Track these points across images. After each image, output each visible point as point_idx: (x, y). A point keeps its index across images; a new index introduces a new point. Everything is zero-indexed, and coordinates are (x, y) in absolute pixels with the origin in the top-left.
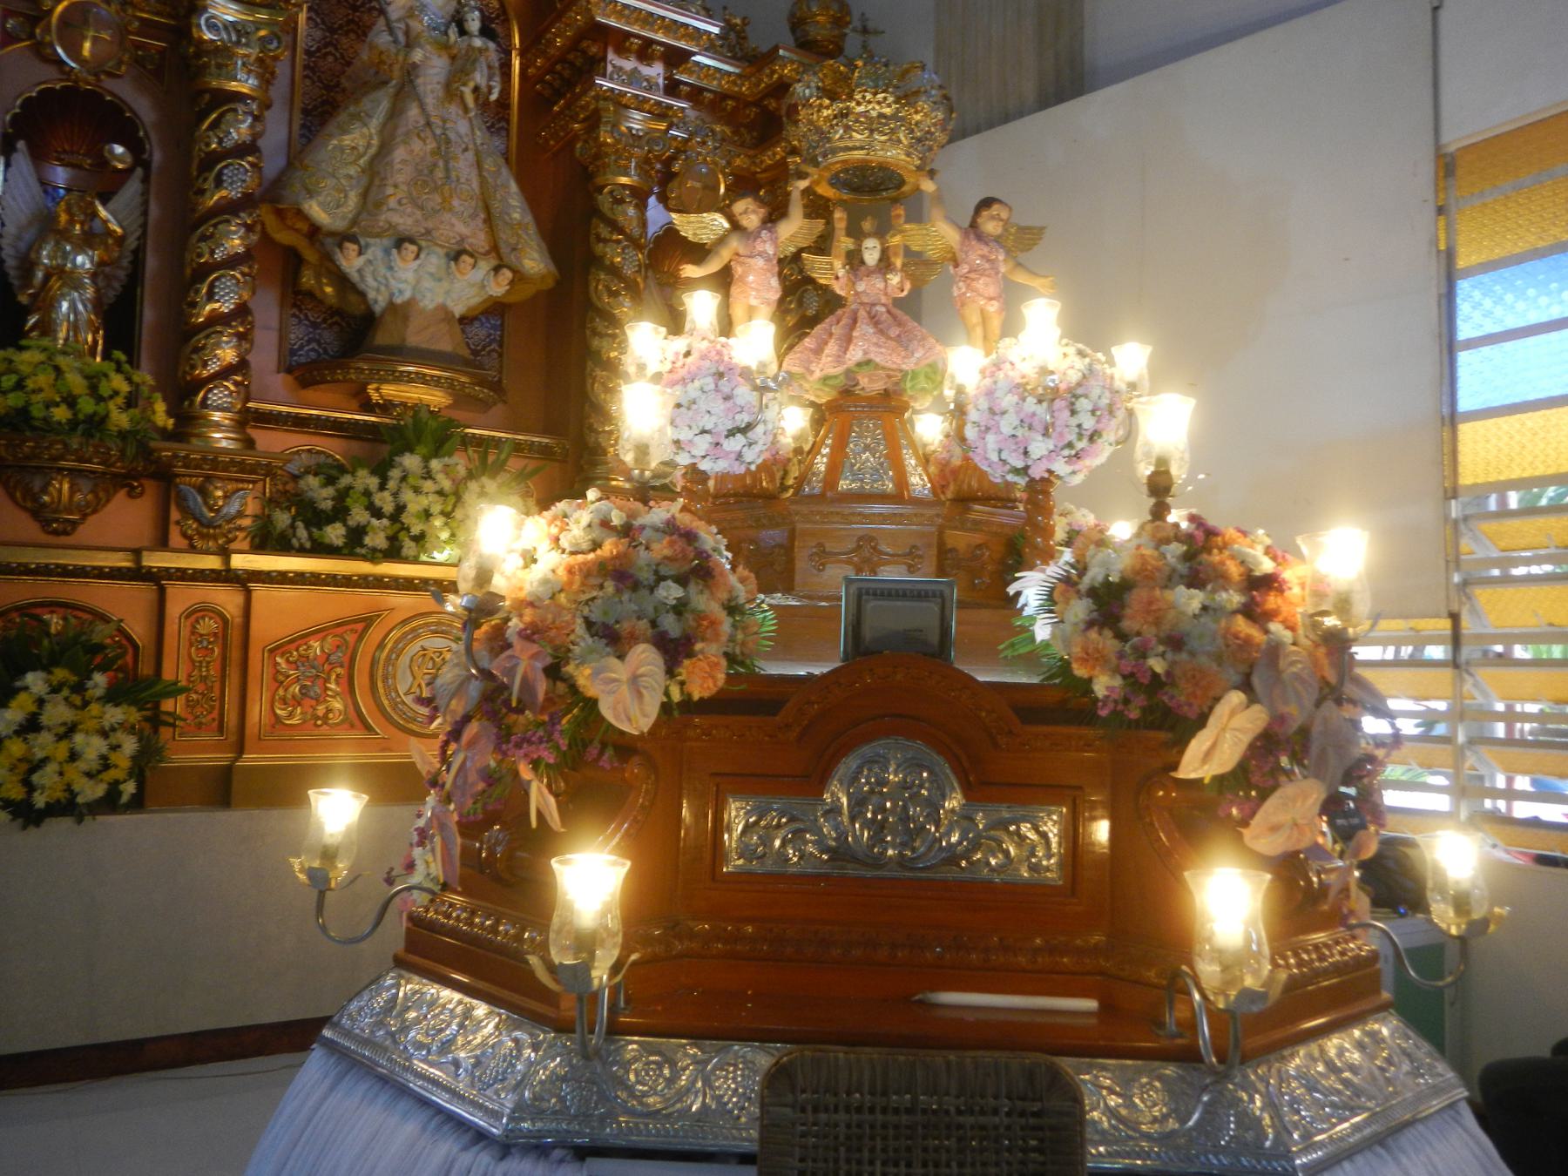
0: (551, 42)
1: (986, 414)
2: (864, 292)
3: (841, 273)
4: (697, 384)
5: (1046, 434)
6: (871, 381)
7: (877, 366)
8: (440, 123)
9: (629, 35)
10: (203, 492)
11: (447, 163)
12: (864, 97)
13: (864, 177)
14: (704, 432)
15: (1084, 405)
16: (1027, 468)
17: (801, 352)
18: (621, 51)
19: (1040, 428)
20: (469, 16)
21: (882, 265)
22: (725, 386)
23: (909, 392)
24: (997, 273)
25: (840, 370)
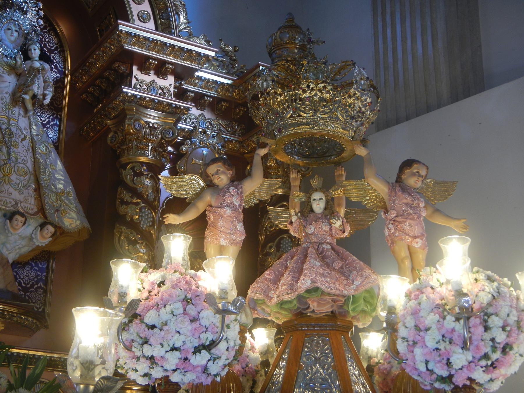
0: (93, 64)
1: (413, 331)
3: (294, 219)
4: (168, 308)
5: (464, 347)
6: (319, 304)
7: (323, 293)
8: (6, 121)
9: (148, 58)
11: (8, 148)
12: (308, 86)
13: (313, 147)
14: (174, 349)
15: (495, 322)
16: (451, 377)
17: (262, 282)
18: (144, 69)
19: (460, 343)
20: (32, 47)
21: (327, 212)
22: (192, 311)
23: (352, 314)
24: (419, 217)
25: (292, 296)
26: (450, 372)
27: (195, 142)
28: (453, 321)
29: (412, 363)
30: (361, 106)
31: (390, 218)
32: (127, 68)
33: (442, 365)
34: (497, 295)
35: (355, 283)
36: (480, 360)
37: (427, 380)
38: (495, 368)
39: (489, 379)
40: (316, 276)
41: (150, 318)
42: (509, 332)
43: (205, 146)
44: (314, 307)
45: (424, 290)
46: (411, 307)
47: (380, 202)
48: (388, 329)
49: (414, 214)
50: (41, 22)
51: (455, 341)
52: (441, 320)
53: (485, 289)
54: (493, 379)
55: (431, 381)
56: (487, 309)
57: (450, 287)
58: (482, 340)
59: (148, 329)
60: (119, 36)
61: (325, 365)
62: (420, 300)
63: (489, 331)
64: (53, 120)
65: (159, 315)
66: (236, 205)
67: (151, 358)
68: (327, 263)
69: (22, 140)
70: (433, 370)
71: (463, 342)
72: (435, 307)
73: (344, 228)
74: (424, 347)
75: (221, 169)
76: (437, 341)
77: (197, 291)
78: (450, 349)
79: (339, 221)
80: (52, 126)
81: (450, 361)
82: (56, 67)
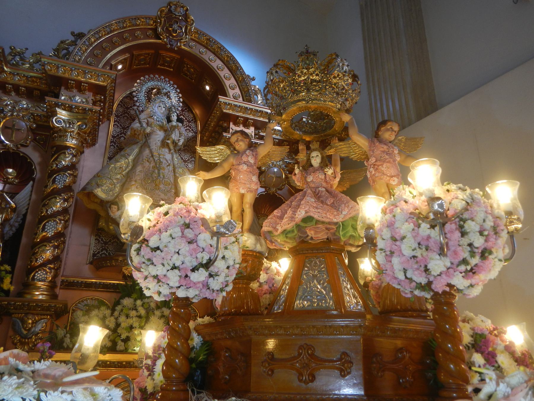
0: (209, 125)
1: (390, 242)
2: (312, 181)
5: (442, 253)
6: (316, 232)
7: (317, 222)
8: (158, 156)
10: (23, 322)
11: (159, 170)
12: (302, 72)
14: (174, 268)
15: (471, 226)
16: (429, 283)
17: (272, 218)
18: (236, 124)
19: (436, 249)
20: (172, 115)
22: (190, 234)
24: (394, 161)
26: (429, 279)
28: (428, 228)
29: (391, 273)
32: (227, 124)
33: (420, 272)
34: (471, 202)
36: (458, 266)
37: (407, 288)
38: (474, 273)
39: (469, 284)
40: (309, 208)
41: (153, 242)
42: (487, 236)
43: (275, 166)
45: (398, 204)
46: (386, 220)
47: (363, 155)
48: (368, 244)
50: (181, 104)
51: (432, 248)
52: (416, 228)
53: (458, 197)
54: (473, 284)
55: (411, 289)
56: (462, 214)
57: (423, 198)
58: (460, 246)
59: (152, 252)
60: (220, 105)
61: (321, 280)
63: (466, 236)
64: (191, 158)
65: (160, 239)
66: (251, 163)
67: (156, 277)
68: (322, 201)
69: (167, 166)
70: (412, 279)
71: (440, 248)
72: (409, 218)
73: (335, 175)
74: (401, 256)
75: (240, 138)
76: (413, 248)
77: (195, 217)
78: (427, 255)
80: (191, 162)
81: (428, 268)
82: (192, 130)
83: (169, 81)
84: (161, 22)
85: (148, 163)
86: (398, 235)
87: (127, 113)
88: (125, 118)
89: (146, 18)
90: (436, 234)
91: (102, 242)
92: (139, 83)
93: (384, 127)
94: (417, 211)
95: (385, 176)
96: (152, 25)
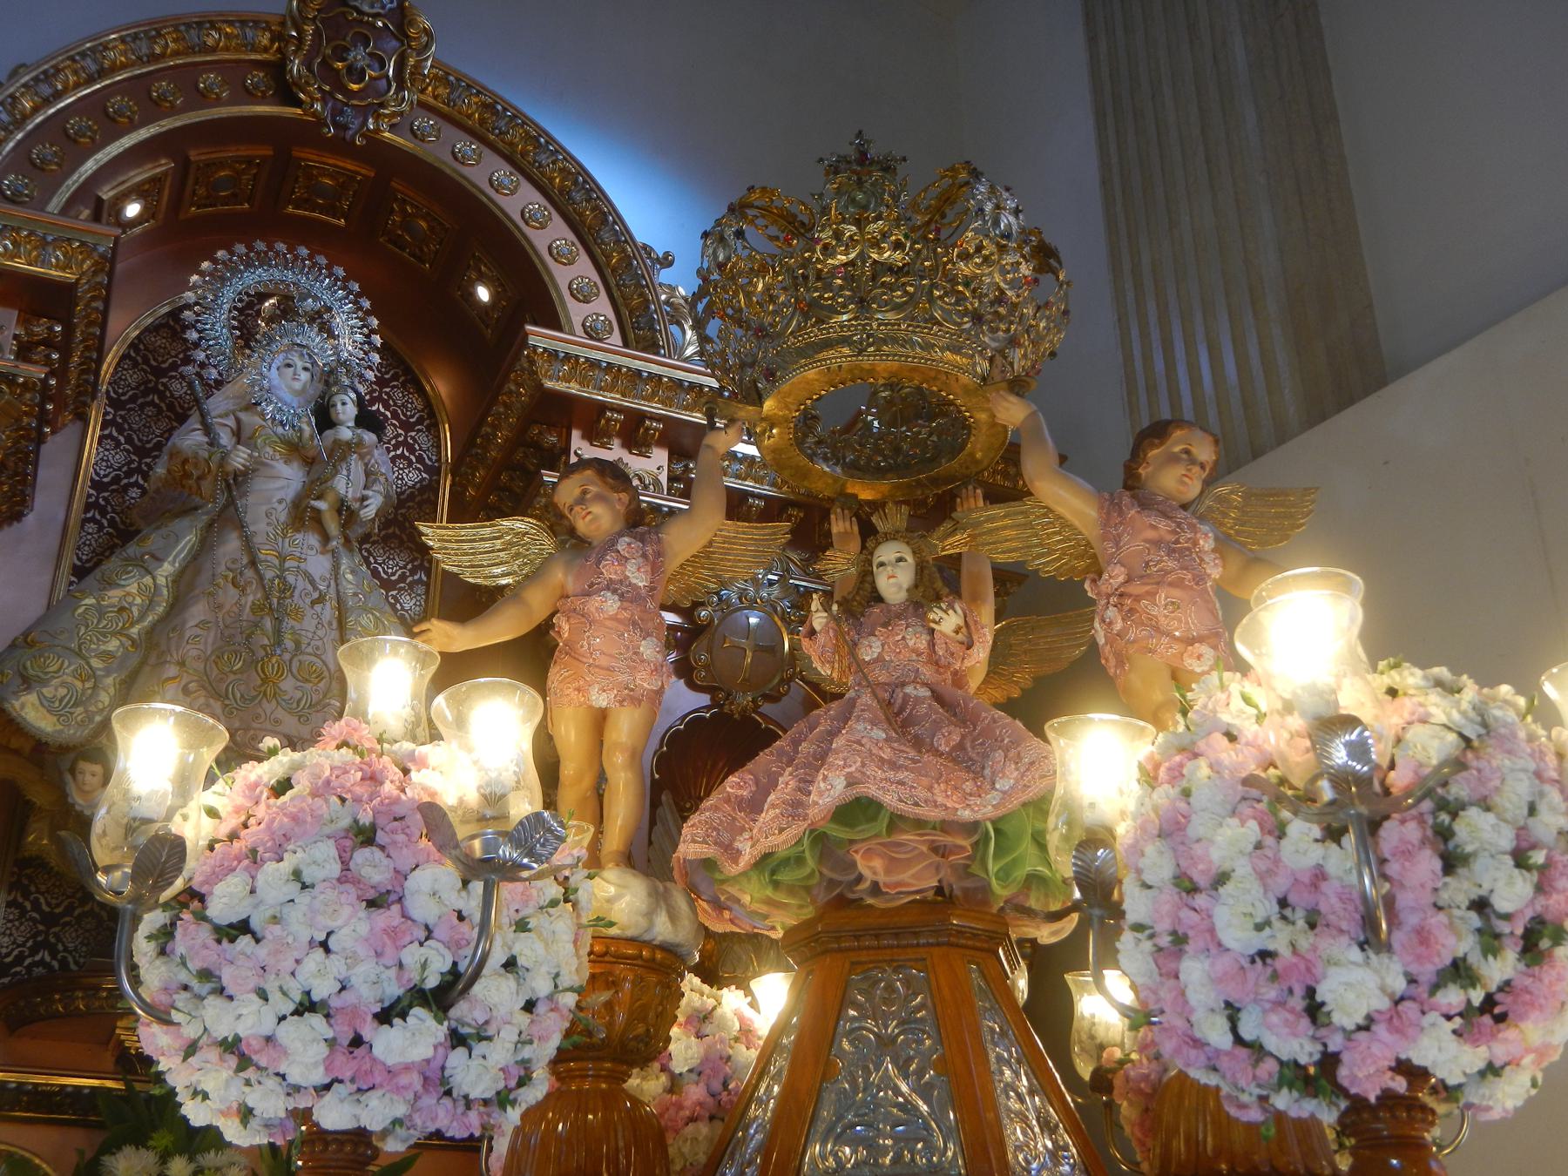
0: (488, 439)
1: (1169, 895)
5: (1371, 939)
6: (893, 864)
7: (897, 822)
8: (276, 562)
9: (603, 407)
11: (279, 621)
12: (838, 235)
14: (307, 1006)
16: (1330, 1061)
17: (716, 808)
19: (1349, 921)
20: (338, 399)
22: (373, 867)
24: (1200, 579)
26: (1325, 1045)
27: (729, 598)
28: (1317, 841)
29: (1179, 1023)
30: (1002, 284)
31: (1109, 591)
32: (559, 436)
33: (1290, 1017)
34: (1479, 736)
35: (998, 786)
36: (1435, 988)
37: (1242, 1083)
38: (1501, 1019)
39: (1481, 1065)
40: (863, 765)
42: (1543, 869)
43: (752, 605)
44: (875, 873)
45: (1202, 745)
46: (1155, 809)
47: (1080, 557)
48: (1091, 906)
49: (1181, 568)
50: (376, 358)
51: (1332, 918)
52: (1269, 841)
53: (1429, 715)
54: (1498, 1063)
55: (1259, 1086)
56: (1445, 784)
57: (1296, 722)
58: (1440, 908)
59: (219, 942)
60: (532, 362)
61: (909, 1060)
62: (1189, 781)
63: (1461, 871)
64: (413, 572)
66: (635, 587)
67: (231, 1046)
68: (916, 737)
69: (313, 603)
70: (1261, 1047)
71: (1363, 917)
72: (1244, 799)
74: (1214, 951)
75: (593, 489)
76: (1258, 920)
77: (397, 801)
78: (1314, 949)
79: (950, 612)
80: (411, 585)
81: (1319, 998)
82: (420, 459)
83: (329, 267)
84: (300, 40)
85: (233, 591)
86: (1201, 867)
87: (155, 390)
88: (150, 410)
89: (243, 23)
90: (1349, 865)
91: (34, 915)
92: (210, 274)
93: (1158, 447)
94: (1272, 771)
95: (1165, 640)
96: (266, 50)
